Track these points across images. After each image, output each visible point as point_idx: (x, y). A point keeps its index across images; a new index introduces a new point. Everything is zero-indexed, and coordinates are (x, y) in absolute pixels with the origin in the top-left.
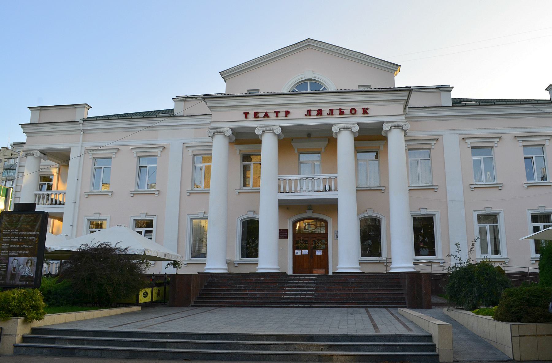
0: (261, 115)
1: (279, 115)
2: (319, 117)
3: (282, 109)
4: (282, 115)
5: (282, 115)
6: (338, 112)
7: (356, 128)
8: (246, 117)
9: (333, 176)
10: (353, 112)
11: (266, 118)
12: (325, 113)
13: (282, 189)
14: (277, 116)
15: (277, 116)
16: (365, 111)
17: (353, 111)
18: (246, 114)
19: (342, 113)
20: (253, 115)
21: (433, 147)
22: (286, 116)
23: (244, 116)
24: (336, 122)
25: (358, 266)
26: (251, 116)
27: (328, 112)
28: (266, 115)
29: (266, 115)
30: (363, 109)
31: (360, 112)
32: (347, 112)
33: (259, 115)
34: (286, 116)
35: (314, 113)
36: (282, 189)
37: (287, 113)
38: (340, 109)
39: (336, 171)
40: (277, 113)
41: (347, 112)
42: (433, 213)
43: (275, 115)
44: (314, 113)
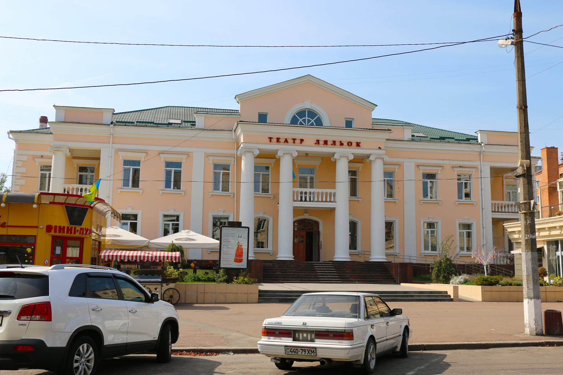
0: (282, 140)
1: (296, 141)
2: (325, 145)
3: (298, 137)
4: (298, 141)
5: (298, 141)
6: (339, 143)
7: (352, 157)
8: (270, 141)
9: (332, 191)
10: (350, 144)
11: (286, 143)
12: (329, 143)
13: (295, 199)
14: (294, 142)
15: (294, 142)
16: (358, 144)
17: (350, 144)
18: (271, 139)
19: (342, 144)
20: (276, 140)
21: (396, 171)
22: (301, 143)
23: (269, 140)
24: (337, 150)
25: (349, 257)
26: (274, 140)
27: (332, 143)
28: (286, 141)
29: (286, 141)
30: (357, 143)
31: (354, 144)
32: (345, 144)
33: (280, 140)
34: (301, 143)
35: (322, 142)
36: (295, 199)
37: (302, 140)
38: (341, 142)
39: (334, 188)
40: (294, 140)
41: (345, 144)
42: (394, 219)
43: (292, 141)
44: (322, 142)
